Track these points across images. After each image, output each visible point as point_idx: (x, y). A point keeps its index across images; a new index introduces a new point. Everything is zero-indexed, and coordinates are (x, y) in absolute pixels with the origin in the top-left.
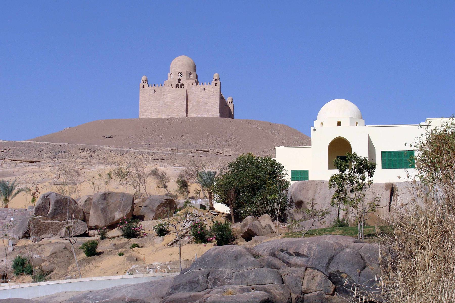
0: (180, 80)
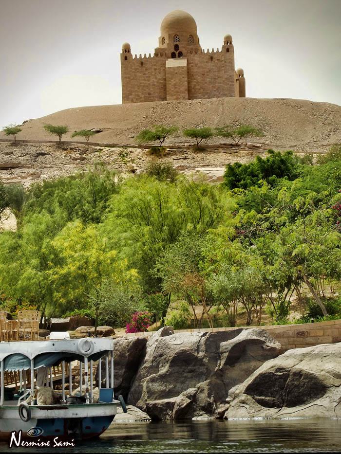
0: (176, 47)
